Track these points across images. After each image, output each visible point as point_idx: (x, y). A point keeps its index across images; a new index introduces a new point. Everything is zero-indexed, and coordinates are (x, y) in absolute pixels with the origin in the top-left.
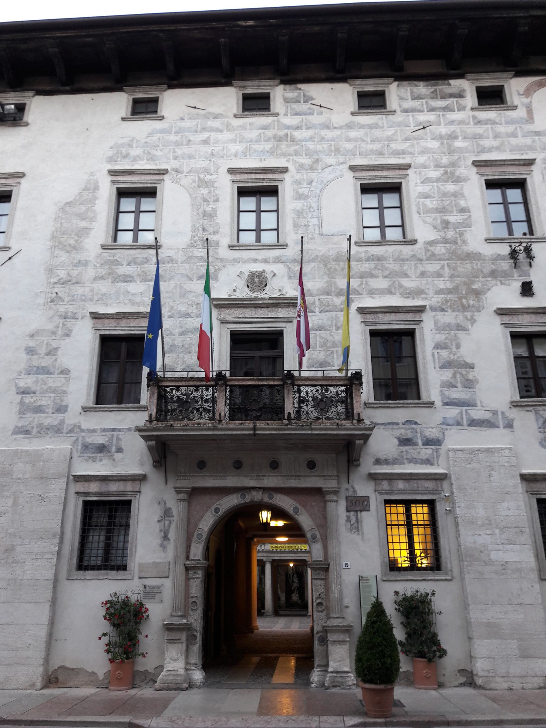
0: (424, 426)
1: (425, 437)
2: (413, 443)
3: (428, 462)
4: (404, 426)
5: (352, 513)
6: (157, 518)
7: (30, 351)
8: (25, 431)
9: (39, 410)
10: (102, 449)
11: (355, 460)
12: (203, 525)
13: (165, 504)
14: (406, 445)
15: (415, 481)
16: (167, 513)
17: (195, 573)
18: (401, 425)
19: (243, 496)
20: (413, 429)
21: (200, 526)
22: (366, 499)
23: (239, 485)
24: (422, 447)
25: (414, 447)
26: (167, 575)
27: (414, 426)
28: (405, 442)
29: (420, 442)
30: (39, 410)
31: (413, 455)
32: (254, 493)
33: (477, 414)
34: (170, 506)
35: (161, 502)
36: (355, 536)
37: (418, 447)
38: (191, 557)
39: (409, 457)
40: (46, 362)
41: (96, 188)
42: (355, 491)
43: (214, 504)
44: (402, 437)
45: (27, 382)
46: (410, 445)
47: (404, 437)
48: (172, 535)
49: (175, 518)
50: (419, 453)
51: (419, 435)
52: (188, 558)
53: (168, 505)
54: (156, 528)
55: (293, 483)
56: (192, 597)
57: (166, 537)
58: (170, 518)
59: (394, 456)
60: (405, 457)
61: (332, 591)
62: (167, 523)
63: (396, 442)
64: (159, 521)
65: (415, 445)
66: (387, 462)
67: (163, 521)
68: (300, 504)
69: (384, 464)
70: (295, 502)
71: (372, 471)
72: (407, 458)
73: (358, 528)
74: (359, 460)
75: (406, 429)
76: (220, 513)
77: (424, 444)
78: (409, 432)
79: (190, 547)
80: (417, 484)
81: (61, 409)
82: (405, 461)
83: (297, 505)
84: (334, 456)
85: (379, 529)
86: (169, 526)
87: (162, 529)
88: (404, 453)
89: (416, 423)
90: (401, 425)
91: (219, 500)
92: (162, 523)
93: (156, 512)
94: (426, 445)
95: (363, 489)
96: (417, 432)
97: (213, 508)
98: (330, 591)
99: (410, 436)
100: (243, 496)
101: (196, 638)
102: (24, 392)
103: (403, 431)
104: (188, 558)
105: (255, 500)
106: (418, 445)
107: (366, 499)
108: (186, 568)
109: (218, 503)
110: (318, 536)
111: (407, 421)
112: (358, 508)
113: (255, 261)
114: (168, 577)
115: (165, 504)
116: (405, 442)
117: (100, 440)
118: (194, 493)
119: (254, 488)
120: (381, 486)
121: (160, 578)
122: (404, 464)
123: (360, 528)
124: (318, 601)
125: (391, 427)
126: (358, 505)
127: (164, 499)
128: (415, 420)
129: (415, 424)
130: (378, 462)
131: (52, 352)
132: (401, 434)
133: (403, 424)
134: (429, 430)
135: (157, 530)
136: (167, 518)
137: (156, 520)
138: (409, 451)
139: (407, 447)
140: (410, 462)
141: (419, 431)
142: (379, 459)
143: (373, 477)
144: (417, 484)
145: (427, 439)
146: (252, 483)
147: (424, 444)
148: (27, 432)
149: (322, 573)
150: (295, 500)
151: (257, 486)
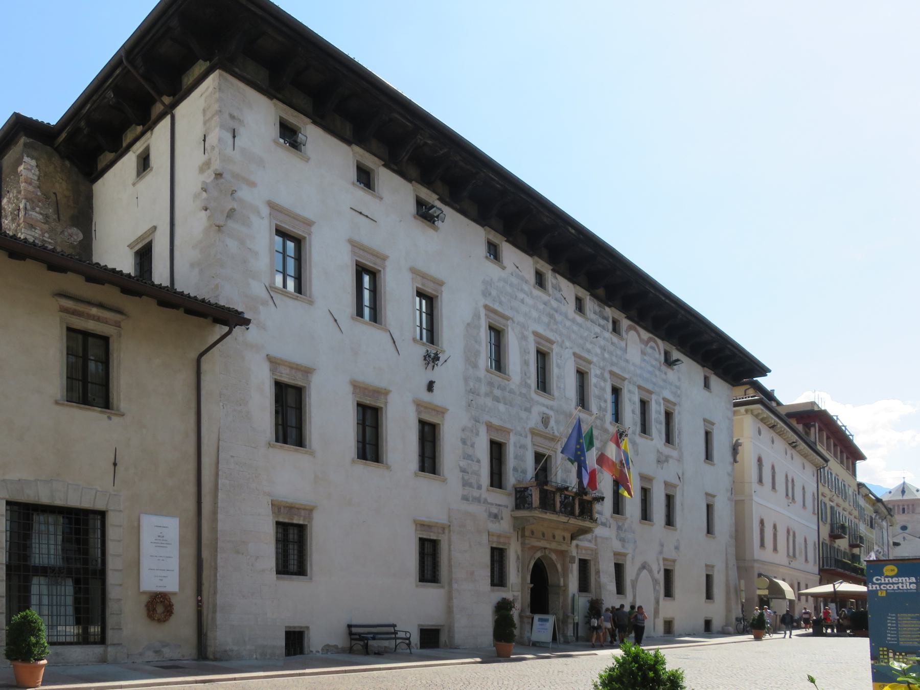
3: (590, 541)
7: (464, 442)
8: (465, 498)
9: (471, 485)
10: (496, 516)
16: (518, 558)
30: (471, 485)
33: (604, 520)
40: (470, 451)
41: (479, 318)
45: (463, 463)
81: (479, 487)
95: (574, 552)
102: (463, 471)
113: (544, 405)
117: (495, 510)
131: (472, 446)
143: (577, 546)
148: (467, 500)
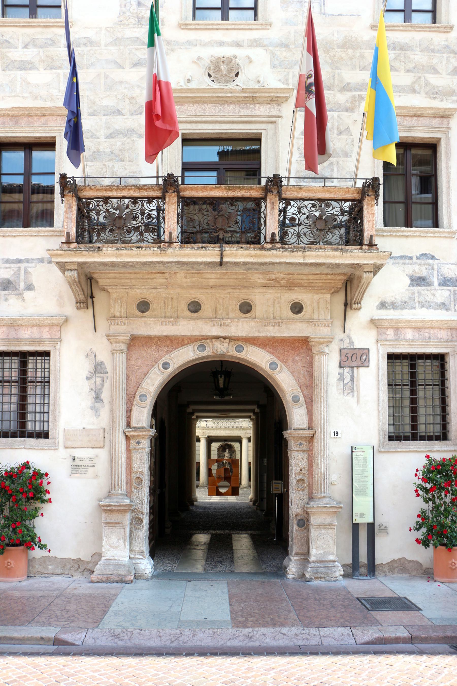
0: (442, 261)
1: (442, 275)
2: (427, 283)
4: (419, 261)
5: (347, 370)
6: (85, 374)
11: (355, 303)
12: (148, 384)
13: (95, 357)
14: (418, 285)
15: (427, 330)
16: (98, 368)
17: (138, 443)
18: (415, 259)
19: (202, 348)
20: (429, 264)
21: (144, 385)
22: (365, 352)
23: (196, 333)
24: (438, 288)
25: (429, 288)
26: (102, 445)
27: (431, 261)
28: (419, 281)
29: (436, 283)
31: (427, 298)
32: (217, 344)
34: (102, 360)
35: (91, 354)
36: (349, 398)
37: (432, 288)
38: (133, 423)
39: (422, 299)
42: (351, 343)
43: (162, 357)
44: (415, 274)
46: (424, 285)
47: (418, 275)
48: (105, 395)
49: (109, 375)
50: (434, 295)
51: (435, 273)
52: (128, 425)
53: (100, 358)
54: (86, 386)
55: (272, 331)
56: (136, 472)
57: (98, 398)
58: (102, 375)
59: (404, 299)
60: (416, 300)
61: (318, 465)
62: (99, 380)
63: (408, 281)
64: (88, 378)
65: (430, 285)
66: (393, 306)
67: (94, 378)
68: (279, 358)
69: (390, 309)
70: (272, 357)
71: (376, 318)
72: (419, 302)
73: (353, 388)
74: (360, 303)
75: (420, 265)
76: (170, 370)
77: (440, 285)
78: (423, 268)
79: (130, 411)
80: (430, 333)
82: (417, 305)
83: (276, 360)
84: (328, 296)
85: (378, 389)
86: (102, 385)
87: (93, 388)
88: (417, 295)
89: (433, 258)
90: (415, 259)
91: (168, 352)
92: (93, 381)
93: (86, 367)
94: (443, 285)
96: (433, 269)
97: (161, 363)
98: (314, 465)
99: (424, 273)
100: (202, 348)
101: (142, 521)
103: (416, 267)
104: (128, 425)
105: (219, 353)
106: (433, 285)
107: (365, 352)
108: (127, 436)
109: (167, 356)
110: (302, 399)
111: (422, 254)
112: (354, 364)
114: (103, 447)
115: (95, 357)
116: (419, 281)
118: (134, 342)
119: (217, 338)
120: (384, 336)
121: (93, 448)
122: (414, 308)
123: (355, 388)
124: (299, 477)
125: (401, 261)
126: (354, 359)
127: (94, 349)
128: (432, 254)
129: (432, 259)
130: (383, 305)
132: (414, 271)
133: (418, 258)
134: (448, 266)
135: (87, 389)
136: (98, 375)
137: (85, 377)
138: (422, 292)
139: (419, 288)
140: (422, 307)
141: (435, 267)
142: (385, 302)
144: (430, 333)
145: (444, 278)
146: (216, 331)
147: (440, 285)
149: (304, 443)
150: (272, 353)
151: (221, 334)
